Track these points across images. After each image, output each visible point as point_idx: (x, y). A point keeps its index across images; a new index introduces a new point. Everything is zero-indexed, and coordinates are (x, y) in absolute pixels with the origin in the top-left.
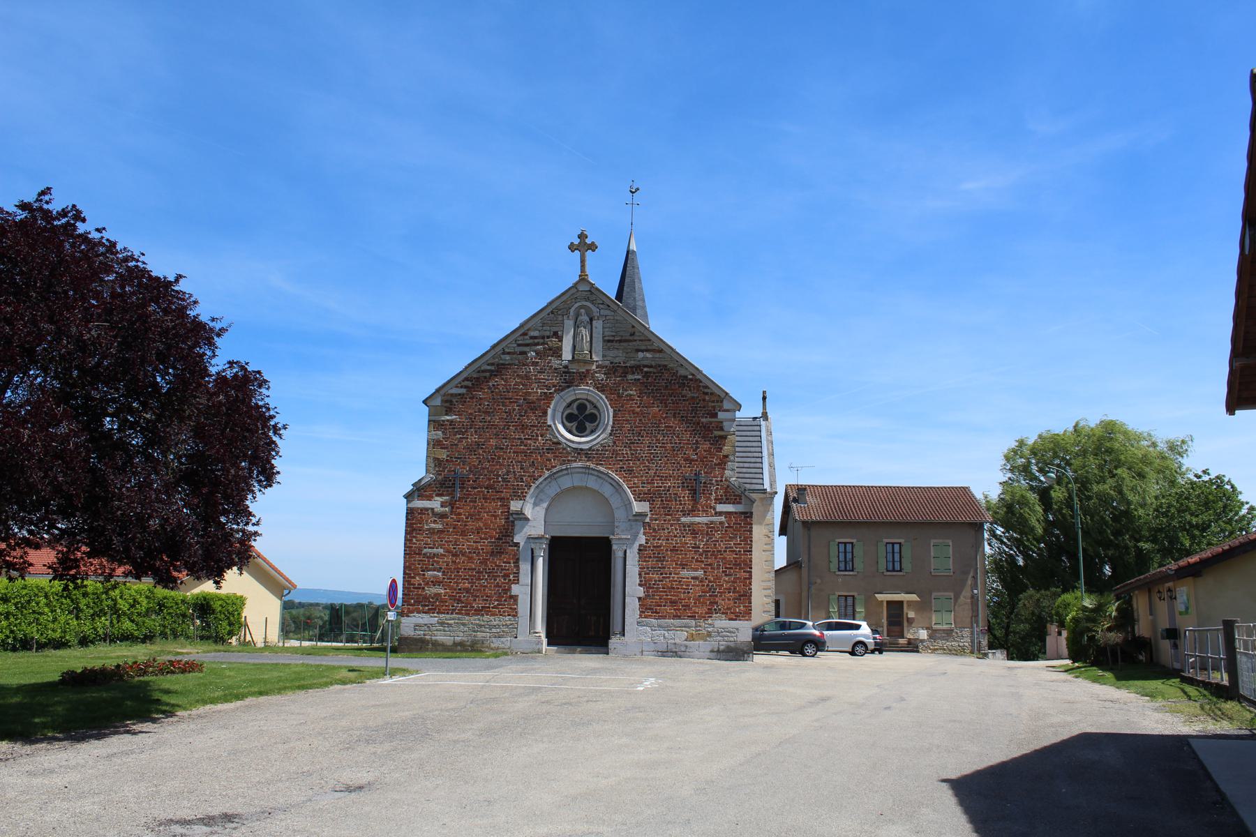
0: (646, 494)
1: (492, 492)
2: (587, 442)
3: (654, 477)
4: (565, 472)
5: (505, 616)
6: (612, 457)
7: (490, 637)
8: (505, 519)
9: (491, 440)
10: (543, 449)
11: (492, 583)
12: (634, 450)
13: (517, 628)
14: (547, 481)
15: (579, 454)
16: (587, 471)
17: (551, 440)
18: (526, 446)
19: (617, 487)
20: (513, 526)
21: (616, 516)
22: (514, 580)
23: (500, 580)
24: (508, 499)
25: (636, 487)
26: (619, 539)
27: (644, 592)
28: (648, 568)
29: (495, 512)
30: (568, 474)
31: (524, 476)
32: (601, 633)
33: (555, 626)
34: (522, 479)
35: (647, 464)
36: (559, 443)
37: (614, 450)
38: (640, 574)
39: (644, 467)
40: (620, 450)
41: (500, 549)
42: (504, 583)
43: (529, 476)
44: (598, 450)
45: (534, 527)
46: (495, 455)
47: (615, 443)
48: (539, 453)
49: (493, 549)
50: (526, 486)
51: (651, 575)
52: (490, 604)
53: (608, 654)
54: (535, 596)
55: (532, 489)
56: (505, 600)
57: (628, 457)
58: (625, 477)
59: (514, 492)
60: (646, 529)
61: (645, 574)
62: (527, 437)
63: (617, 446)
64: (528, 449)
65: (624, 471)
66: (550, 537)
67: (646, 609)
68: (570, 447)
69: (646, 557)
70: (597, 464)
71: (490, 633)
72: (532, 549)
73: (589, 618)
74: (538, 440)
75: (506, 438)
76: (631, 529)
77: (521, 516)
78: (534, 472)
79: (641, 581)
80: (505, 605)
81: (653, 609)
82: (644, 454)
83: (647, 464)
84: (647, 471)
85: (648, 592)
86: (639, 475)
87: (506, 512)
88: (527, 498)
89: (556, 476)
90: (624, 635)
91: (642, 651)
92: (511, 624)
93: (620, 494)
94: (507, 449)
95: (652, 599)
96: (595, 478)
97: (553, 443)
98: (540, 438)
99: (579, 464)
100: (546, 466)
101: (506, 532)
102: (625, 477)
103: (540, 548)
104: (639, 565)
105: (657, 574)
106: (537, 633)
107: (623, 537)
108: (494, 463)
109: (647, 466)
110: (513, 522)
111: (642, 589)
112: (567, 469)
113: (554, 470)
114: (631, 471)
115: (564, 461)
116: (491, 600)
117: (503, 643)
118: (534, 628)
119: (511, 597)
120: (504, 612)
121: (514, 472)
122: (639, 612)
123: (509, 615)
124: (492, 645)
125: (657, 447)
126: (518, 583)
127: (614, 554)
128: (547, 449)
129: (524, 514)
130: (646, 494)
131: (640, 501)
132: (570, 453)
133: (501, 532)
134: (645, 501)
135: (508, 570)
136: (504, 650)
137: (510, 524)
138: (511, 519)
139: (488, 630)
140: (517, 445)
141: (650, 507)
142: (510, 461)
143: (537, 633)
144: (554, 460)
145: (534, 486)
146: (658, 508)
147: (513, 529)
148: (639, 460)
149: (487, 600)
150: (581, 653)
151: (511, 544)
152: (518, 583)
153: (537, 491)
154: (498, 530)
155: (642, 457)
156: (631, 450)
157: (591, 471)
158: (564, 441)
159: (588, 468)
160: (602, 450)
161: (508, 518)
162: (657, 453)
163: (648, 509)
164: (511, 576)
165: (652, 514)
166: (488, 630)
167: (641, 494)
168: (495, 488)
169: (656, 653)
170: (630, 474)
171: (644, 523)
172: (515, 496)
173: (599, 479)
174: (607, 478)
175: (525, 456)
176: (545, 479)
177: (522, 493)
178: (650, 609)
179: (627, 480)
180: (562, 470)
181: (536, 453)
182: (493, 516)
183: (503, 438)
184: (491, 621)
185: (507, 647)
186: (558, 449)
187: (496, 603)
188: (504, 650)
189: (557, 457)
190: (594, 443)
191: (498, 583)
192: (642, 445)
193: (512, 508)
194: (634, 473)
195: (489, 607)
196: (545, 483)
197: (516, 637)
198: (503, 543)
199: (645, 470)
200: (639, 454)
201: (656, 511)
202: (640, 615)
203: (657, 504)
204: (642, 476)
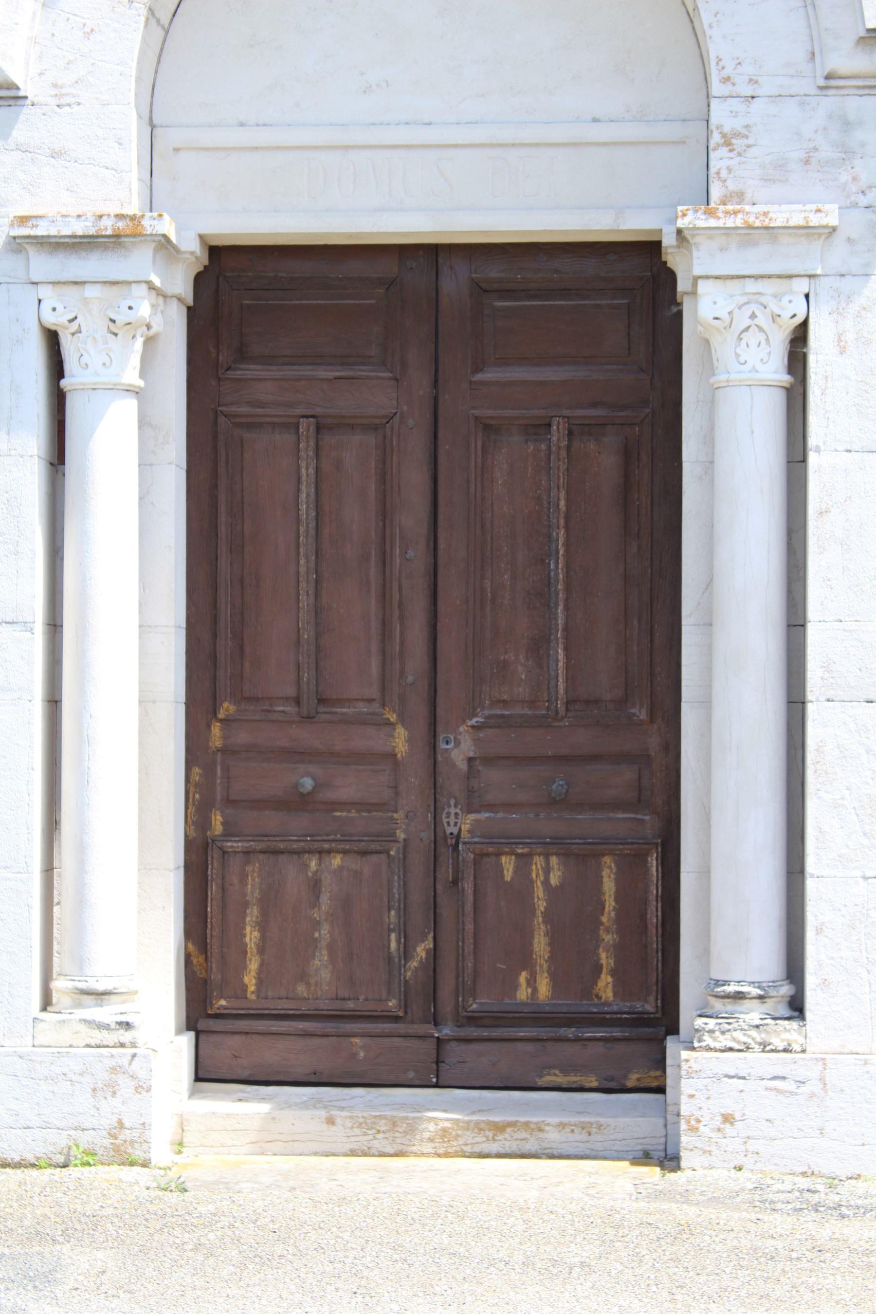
21: (715, 49)
32: (605, 986)
33: (251, 936)
45: (55, 154)
66: (191, 246)
72: (52, 339)
73: (508, 864)
103: (113, 327)
107: (780, 216)
118: (80, 962)
143: (101, 996)
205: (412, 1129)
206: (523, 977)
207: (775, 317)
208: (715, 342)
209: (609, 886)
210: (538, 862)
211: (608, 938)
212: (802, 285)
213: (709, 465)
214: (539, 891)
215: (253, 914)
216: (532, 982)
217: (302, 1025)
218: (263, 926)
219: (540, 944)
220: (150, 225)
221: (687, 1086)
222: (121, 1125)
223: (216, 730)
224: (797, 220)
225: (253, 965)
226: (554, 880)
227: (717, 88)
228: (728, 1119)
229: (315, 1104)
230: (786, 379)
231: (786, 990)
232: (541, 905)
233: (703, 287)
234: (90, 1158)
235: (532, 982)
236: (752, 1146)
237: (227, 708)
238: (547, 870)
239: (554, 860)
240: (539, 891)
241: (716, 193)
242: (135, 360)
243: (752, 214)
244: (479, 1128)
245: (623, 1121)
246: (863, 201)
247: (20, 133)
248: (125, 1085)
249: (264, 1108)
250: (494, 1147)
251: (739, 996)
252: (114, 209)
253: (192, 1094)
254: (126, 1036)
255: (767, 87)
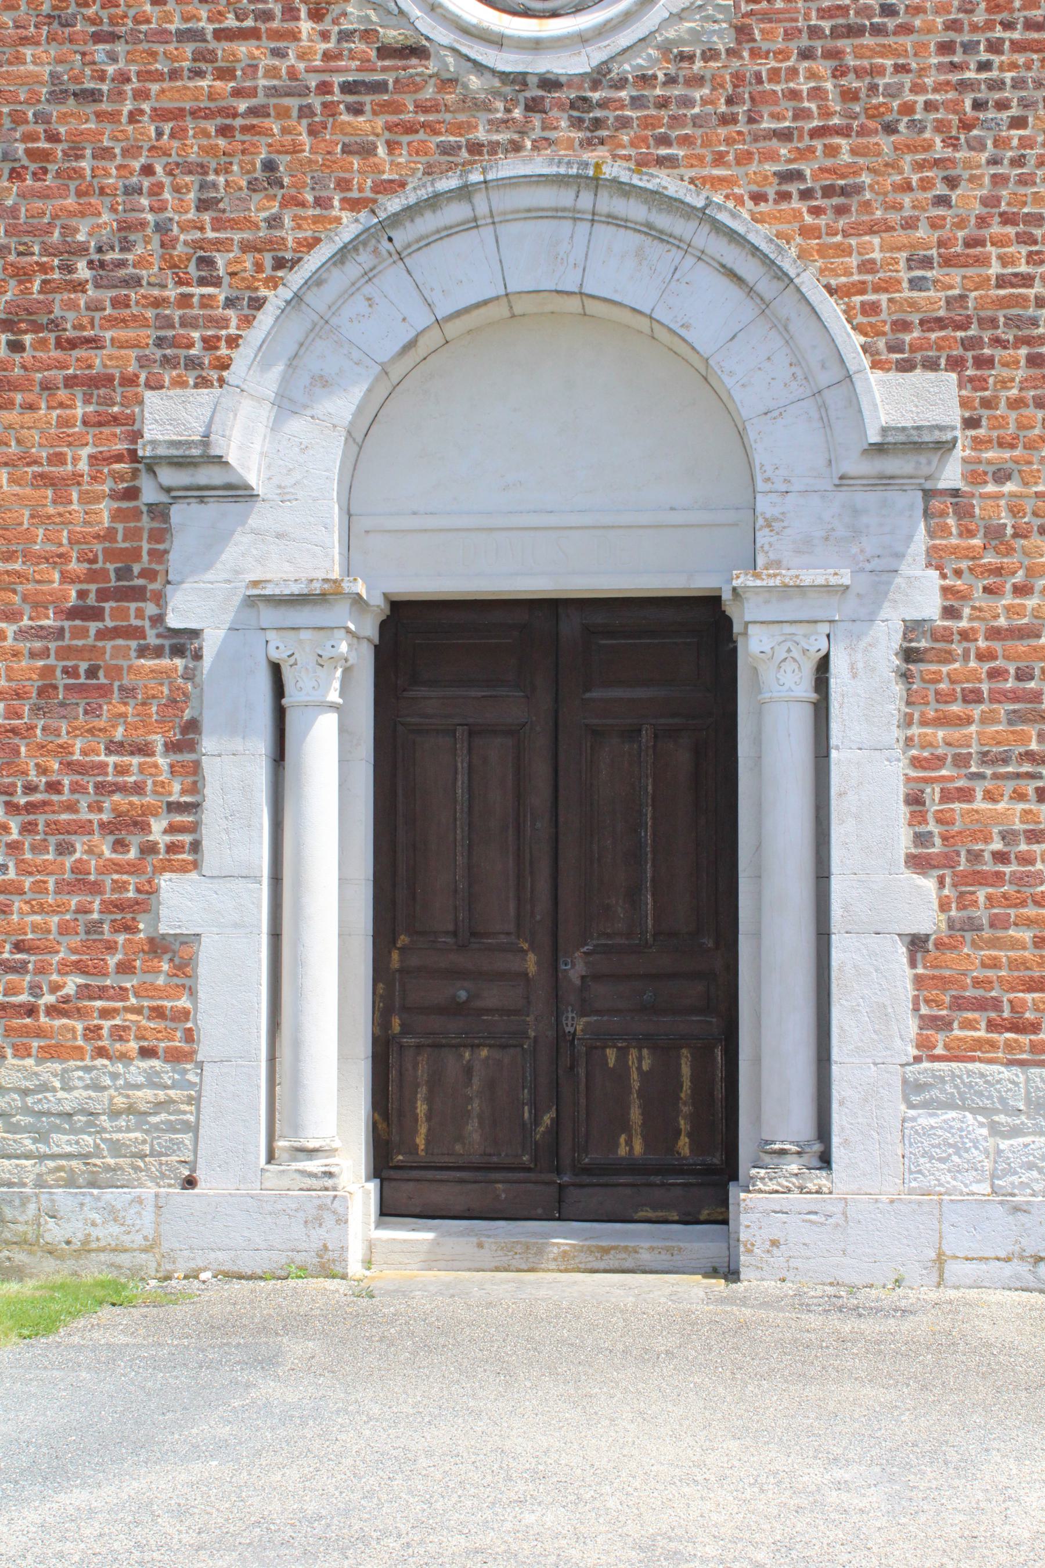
0: (940, 323)
1: (42, 344)
2: (582, 39)
3: (982, 221)
4: (455, 212)
5: (124, 1057)
6: (726, 120)
7: (40, 1183)
8: (115, 496)
9: (28, 52)
10: (324, 88)
11: (43, 869)
12: (859, 72)
13: (194, 1129)
14: (352, 270)
15: (533, 106)
16: (586, 200)
17: (368, 35)
18: (225, 74)
19: (766, 287)
20: (160, 535)
21: (760, 457)
22: (171, 848)
23: (90, 851)
24: (130, 381)
25: (877, 289)
26: (786, 591)
27: (944, 907)
28: (960, 761)
29: (58, 459)
30: (473, 223)
31: (219, 245)
32: (684, 1142)
33: (421, 1108)
34: (206, 262)
35: (939, 150)
36: (416, 51)
37: (738, 78)
38: (914, 800)
39: (919, 166)
40: (774, 75)
41: (92, 673)
42: (118, 867)
43: (247, 247)
44: (645, 80)
45: (279, 536)
46: (53, 138)
47: (742, 32)
48: (306, 111)
49: (47, 672)
50: (230, 303)
51: (980, 804)
52: (35, 990)
53: (732, 1274)
54: (297, 941)
55: (265, 319)
56: (125, 968)
57: (826, 114)
58: (806, 232)
59: (160, 342)
60: (945, 530)
61: (946, 796)
62: (231, 22)
63: (754, 54)
64: (237, 93)
65: (806, 195)
66: (378, 601)
67: (959, 1004)
68: (479, 67)
69: (942, 698)
70: (642, 163)
71: (43, 1157)
72: (276, 670)
73: (611, 1055)
74: (294, 36)
75: (113, 37)
76: (856, 533)
77: (206, 476)
78: (274, 222)
79: (921, 839)
80: (122, 993)
81: (996, 1005)
82: (917, 88)
83: (939, 150)
84: (941, 189)
85: (964, 901)
86: (894, 217)
87: (119, 458)
88: (242, 359)
89: (401, 237)
90: (825, 1161)
91: (940, 1260)
92: (160, 1106)
93: (783, 328)
94: (118, 95)
95: (994, 943)
96: (632, 240)
97: (385, 52)
98: (306, 26)
99: (539, 165)
100: (343, 185)
101: (123, 573)
102: (806, 232)
104: (909, 741)
105: (1020, 796)
106: (311, 1153)
107: (810, 577)
108: (49, 180)
109: (937, 163)
110: (161, 513)
111: (928, 884)
112: (465, 192)
113: (393, 204)
114: (844, 192)
115: (447, 150)
116: (42, 970)
117: (113, 1215)
118: (296, 1128)
119: (157, 946)
120: (119, 1034)
121: (161, 228)
122: (912, 1026)
123: (147, 1053)
124: (54, 1232)
125: (995, 47)
126: (196, 865)
127: (756, 685)
128: (348, 88)
129: (219, 461)
130: (940, 323)
131: (906, 366)
132: (487, 107)
133: (93, 576)
134: (931, 365)
135: (138, 789)
136: (123, 1259)
137: (145, 522)
138: (150, 494)
139: (28, 1144)
140: (174, 74)
141: (964, 403)
142: (137, 165)
143: (311, 1153)
144: (391, 146)
145: (275, 299)
146: (1016, 404)
147: (160, 556)
148: (890, 129)
149: (20, 968)
150: (568, 1264)
151: (152, 639)
152: (196, 865)
153: (297, 327)
154: (73, 566)
155: (908, 109)
156: (839, 72)
157: (609, 203)
158: (442, 35)
159: (595, 183)
160: (671, 80)
161: (132, 494)
162: (996, 85)
163: (954, 416)
164: (157, 826)
165: (978, 443)
166: (28, 1144)
167: (903, 326)
168: (55, 325)
169: (1022, 1269)
170: (841, 211)
171: (929, 494)
172: (166, 361)
173: (655, 250)
174: (703, 238)
175: (224, 131)
176: (342, 256)
177: (210, 344)
178: (980, 1005)
179: (822, 251)
180: (434, 202)
181: (283, 113)
182: (44, 480)
183: (98, 38)
184: (45, 1088)
185: (139, 1240)
186: (414, 86)
187: (72, 983)
188: (123, 1259)
189: (410, 129)
190: (624, 39)
191: (79, 868)
192: (907, 42)
193: (152, 431)
194: (866, 205)
195: (31, 1011)
196: (339, 279)
197: (190, 1183)
198: (101, 635)
199: (926, 184)
200: (892, 92)
201: (999, 423)
202: (924, 1044)
203: (1004, 383)
204: (910, 224)
205: (540, 1252)
206: (623, 1139)
207: (805, 651)
208: (761, 669)
209: (686, 1070)
210: (633, 1053)
211: (685, 1109)
212: (825, 628)
213: (758, 759)
214: (635, 1075)
215: (422, 1092)
216: (629, 1142)
217: (458, 1174)
218: (429, 1100)
219: (635, 1115)
220: (347, 586)
221: (744, 1219)
222: (325, 1248)
223: (395, 956)
224: (821, 581)
225: (423, 1129)
226: (646, 1066)
227: (760, 485)
228: (775, 1243)
229: (467, 1233)
230: (813, 696)
231: (817, 1147)
232: (636, 1085)
233: (752, 630)
234: (304, 1272)
235: (629, 1142)
236: (793, 1263)
237: (403, 940)
238: (640, 1059)
239: (645, 1052)
240: (635, 1075)
241: (761, 561)
242: (336, 684)
243: (787, 576)
244: (590, 1250)
245: (697, 1245)
246: (869, 567)
247: (253, 522)
248: (329, 1220)
249: (430, 1236)
250: (602, 1265)
251: (783, 1152)
252: (321, 575)
253: (378, 1226)
254: (329, 1183)
255: (797, 486)
